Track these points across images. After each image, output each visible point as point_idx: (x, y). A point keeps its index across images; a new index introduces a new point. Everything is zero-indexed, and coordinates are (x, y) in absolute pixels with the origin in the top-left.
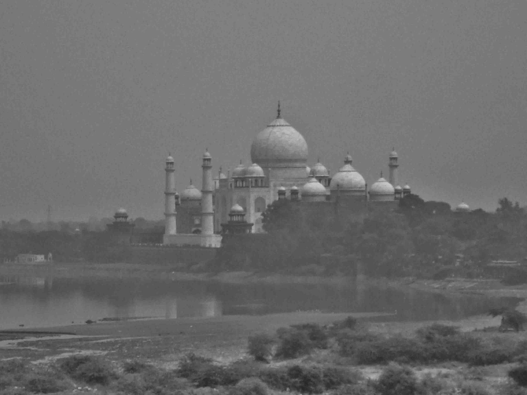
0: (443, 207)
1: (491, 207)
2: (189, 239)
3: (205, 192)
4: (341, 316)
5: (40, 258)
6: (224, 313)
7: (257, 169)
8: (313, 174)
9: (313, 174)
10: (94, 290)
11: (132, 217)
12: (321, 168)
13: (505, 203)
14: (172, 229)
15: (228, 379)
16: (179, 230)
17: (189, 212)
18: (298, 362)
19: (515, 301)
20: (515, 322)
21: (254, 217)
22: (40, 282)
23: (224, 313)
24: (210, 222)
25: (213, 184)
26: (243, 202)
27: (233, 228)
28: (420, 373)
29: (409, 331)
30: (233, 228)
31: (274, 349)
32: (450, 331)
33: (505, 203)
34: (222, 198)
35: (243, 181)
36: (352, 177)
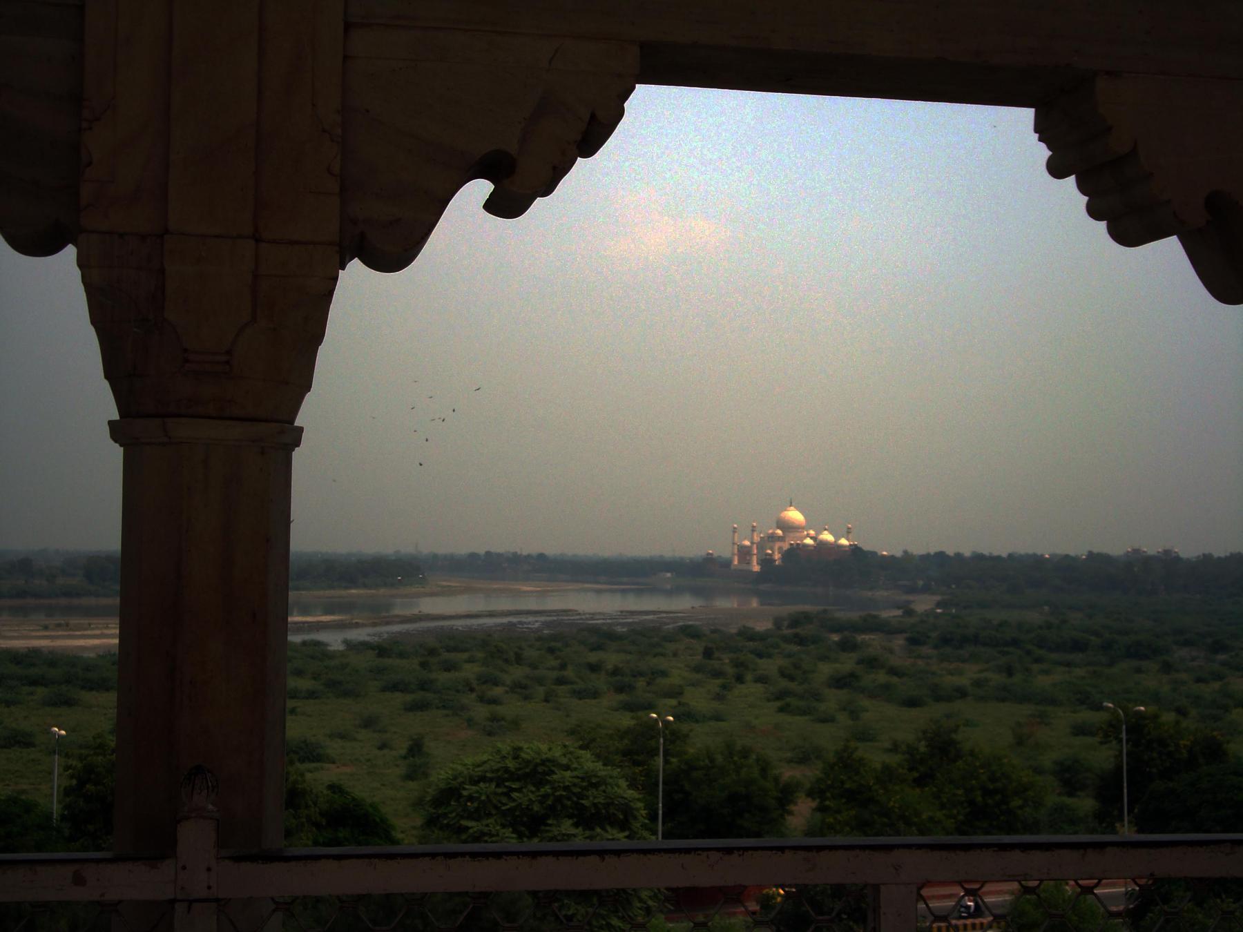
0: (874, 554)
1: (899, 554)
2: (744, 567)
3: (752, 543)
4: (821, 608)
5: (669, 575)
6: (762, 604)
7: (779, 532)
8: (808, 536)
9: (808, 536)
10: (697, 592)
11: (716, 555)
12: (812, 532)
13: (905, 552)
14: (736, 562)
15: (762, 637)
16: (739, 561)
17: (744, 553)
18: (798, 630)
19: (909, 602)
20: (909, 612)
21: (777, 556)
22: (669, 587)
23: (762, 604)
24: (755, 559)
25: (756, 539)
26: (771, 549)
27: (766, 562)
28: (860, 638)
29: (854, 615)
30: (766, 562)
31: (786, 623)
32: (875, 617)
33: (905, 552)
34: (761, 546)
35: (773, 538)
36: (827, 537)
